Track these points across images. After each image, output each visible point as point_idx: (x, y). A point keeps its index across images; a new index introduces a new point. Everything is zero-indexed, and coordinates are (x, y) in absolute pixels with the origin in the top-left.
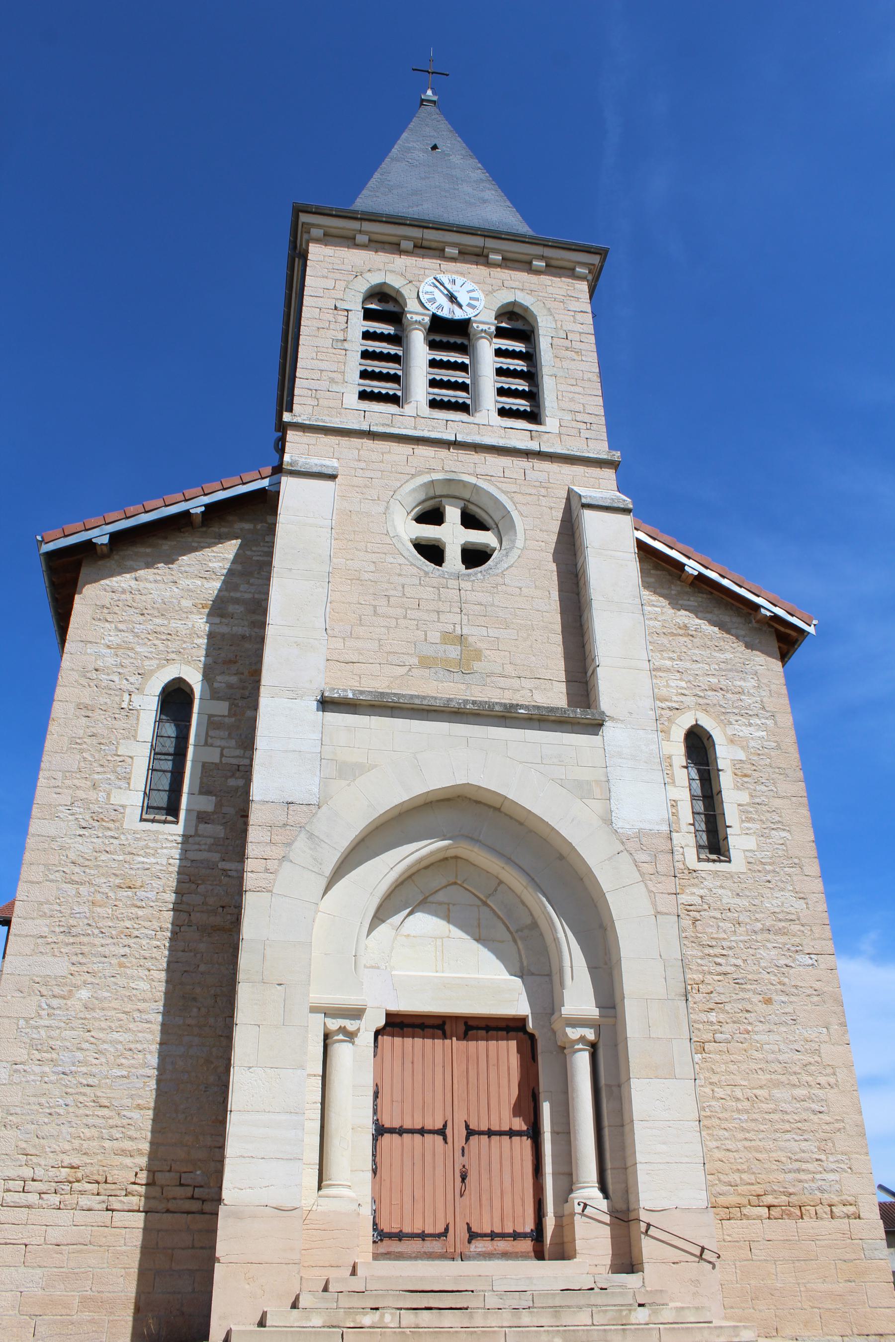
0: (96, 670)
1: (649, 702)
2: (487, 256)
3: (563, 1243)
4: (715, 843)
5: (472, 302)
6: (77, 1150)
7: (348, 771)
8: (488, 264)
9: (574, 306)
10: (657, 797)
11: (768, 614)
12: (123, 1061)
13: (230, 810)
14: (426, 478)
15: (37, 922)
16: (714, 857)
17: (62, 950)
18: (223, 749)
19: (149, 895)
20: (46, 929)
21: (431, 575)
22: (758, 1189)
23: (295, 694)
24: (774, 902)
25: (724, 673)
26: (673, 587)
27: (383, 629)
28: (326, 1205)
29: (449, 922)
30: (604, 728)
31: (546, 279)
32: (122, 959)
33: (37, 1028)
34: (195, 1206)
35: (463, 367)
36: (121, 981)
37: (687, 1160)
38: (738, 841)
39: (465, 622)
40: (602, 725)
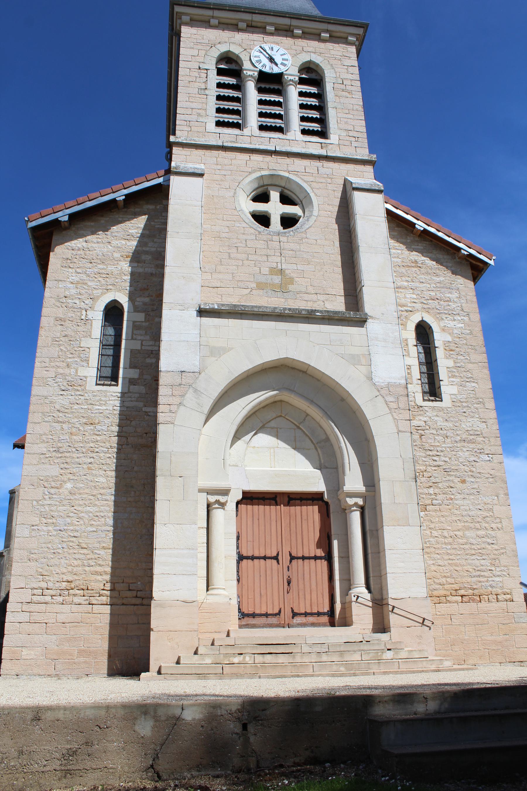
0: (65, 297)
1: (393, 307)
2: (293, 31)
3: (345, 618)
4: (433, 390)
5: (284, 62)
6: (71, 572)
7: (216, 352)
8: (294, 36)
9: (347, 62)
10: (400, 364)
11: (466, 253)
12: (93, 523)
13: (148, 377)
14: (258, 174)
15: (40, 445)
16: (433, 398)
17: (55, 461)
18: (142, 341)
19: (105, 428)
20: (45, 449)
21: (262, 233)
22: (456, 587)
23: (183, 307)
24: (467, 424)
25: (439, 289)
26: (408, 238)
27: (234, 267)
28: (211, 599)
29: (277, 438)
30: (367, 323)
31: (329, 45)
32: (90, 465)
33: (43, 505)
34: (138, 601)
35: (278, 104)
36: (90, 478)
37: (415, 571)
38: (447, 389)
39: (283, 261)
40: (366, 321)
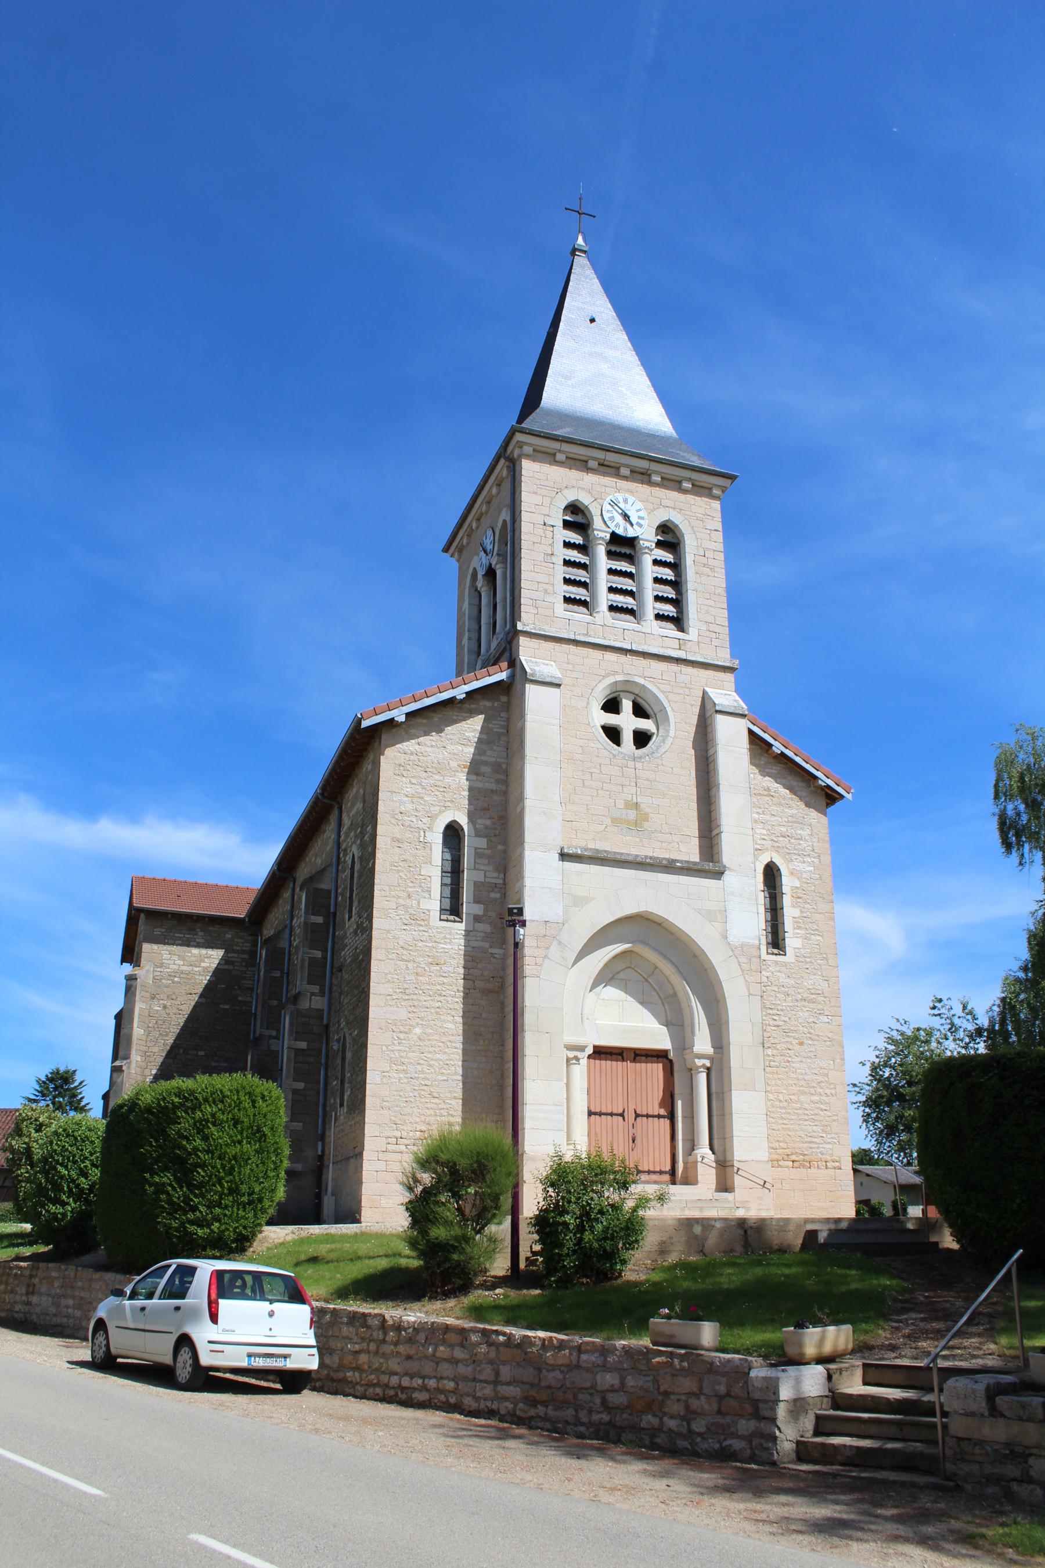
2: (650, 475)
4: (776, 941)
7: (579, 901)
8: (650, 483)
13: (493, 914)
14: (611, 680)
16: (776, 951)
19: (450, 969)
22: (788, 1151)
31: (690, 498)
38: (792, 941)
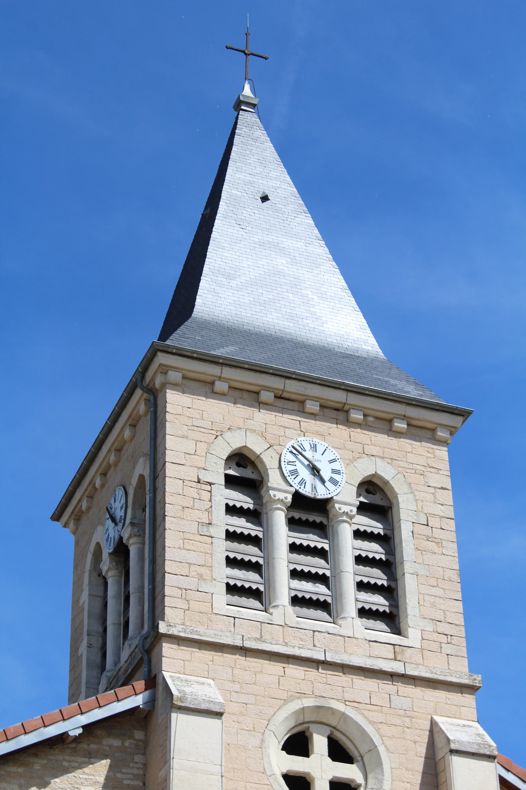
2: (347, 412)
8: (348, 423)
31: (405, 443)
